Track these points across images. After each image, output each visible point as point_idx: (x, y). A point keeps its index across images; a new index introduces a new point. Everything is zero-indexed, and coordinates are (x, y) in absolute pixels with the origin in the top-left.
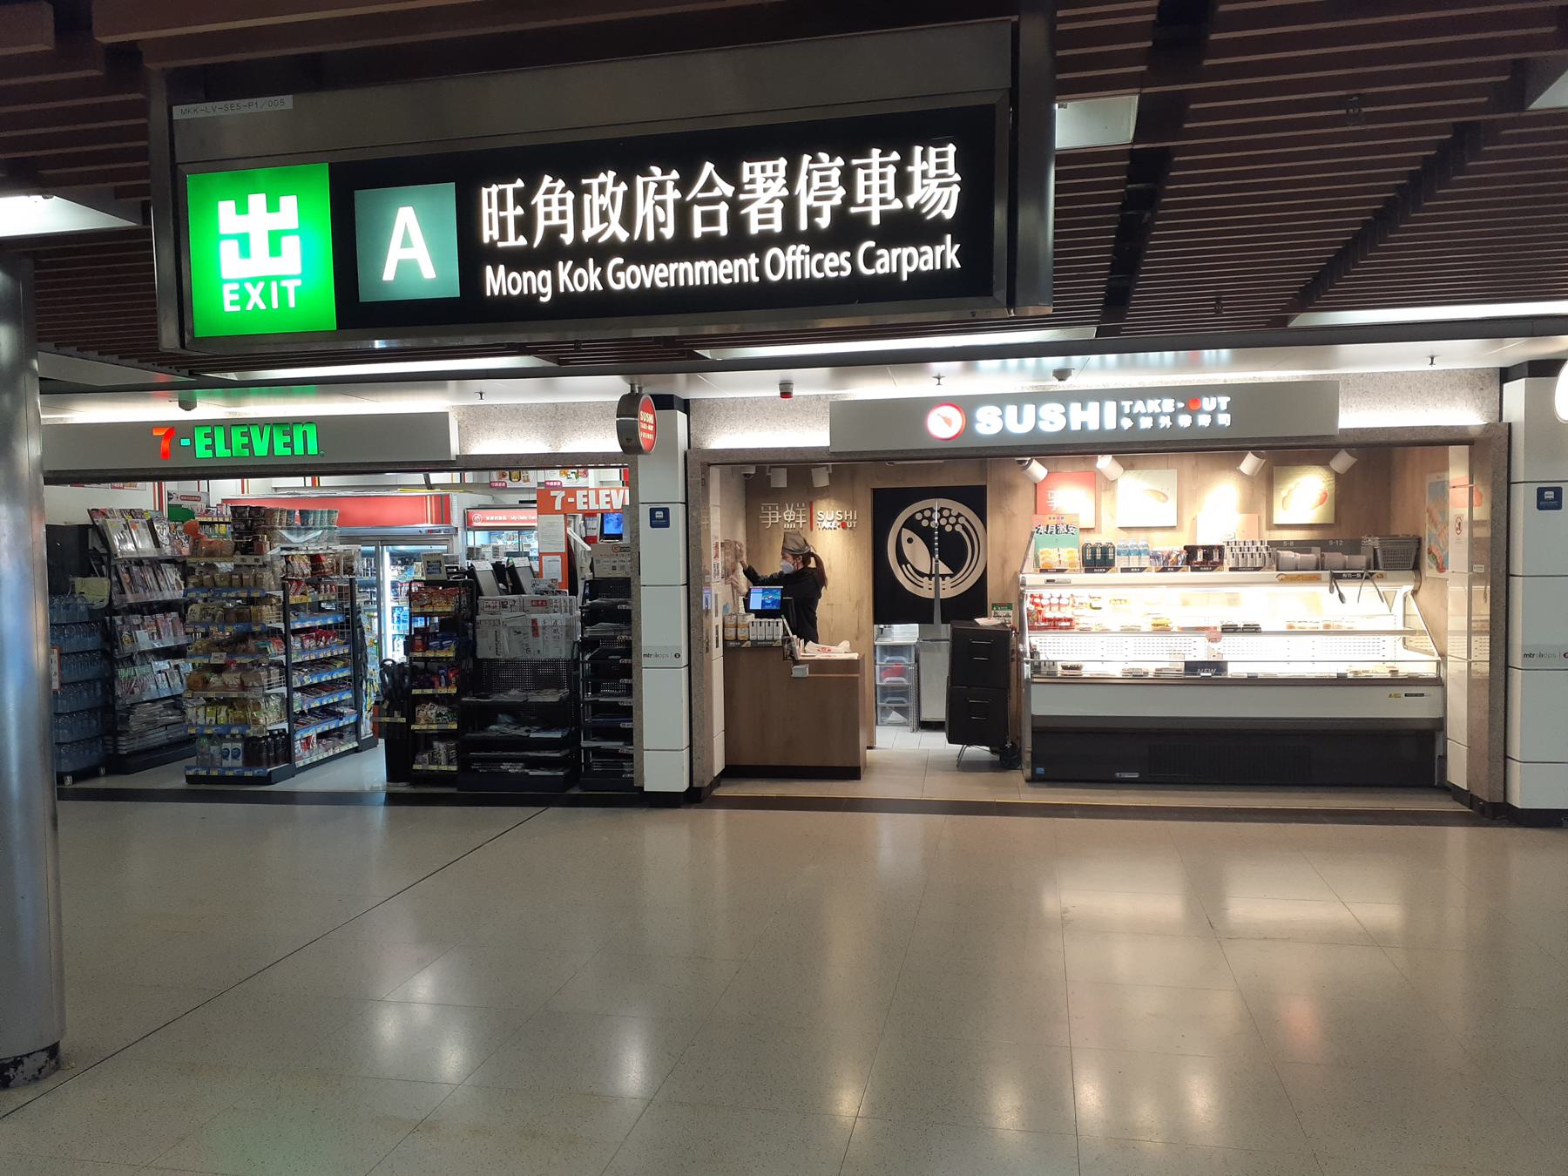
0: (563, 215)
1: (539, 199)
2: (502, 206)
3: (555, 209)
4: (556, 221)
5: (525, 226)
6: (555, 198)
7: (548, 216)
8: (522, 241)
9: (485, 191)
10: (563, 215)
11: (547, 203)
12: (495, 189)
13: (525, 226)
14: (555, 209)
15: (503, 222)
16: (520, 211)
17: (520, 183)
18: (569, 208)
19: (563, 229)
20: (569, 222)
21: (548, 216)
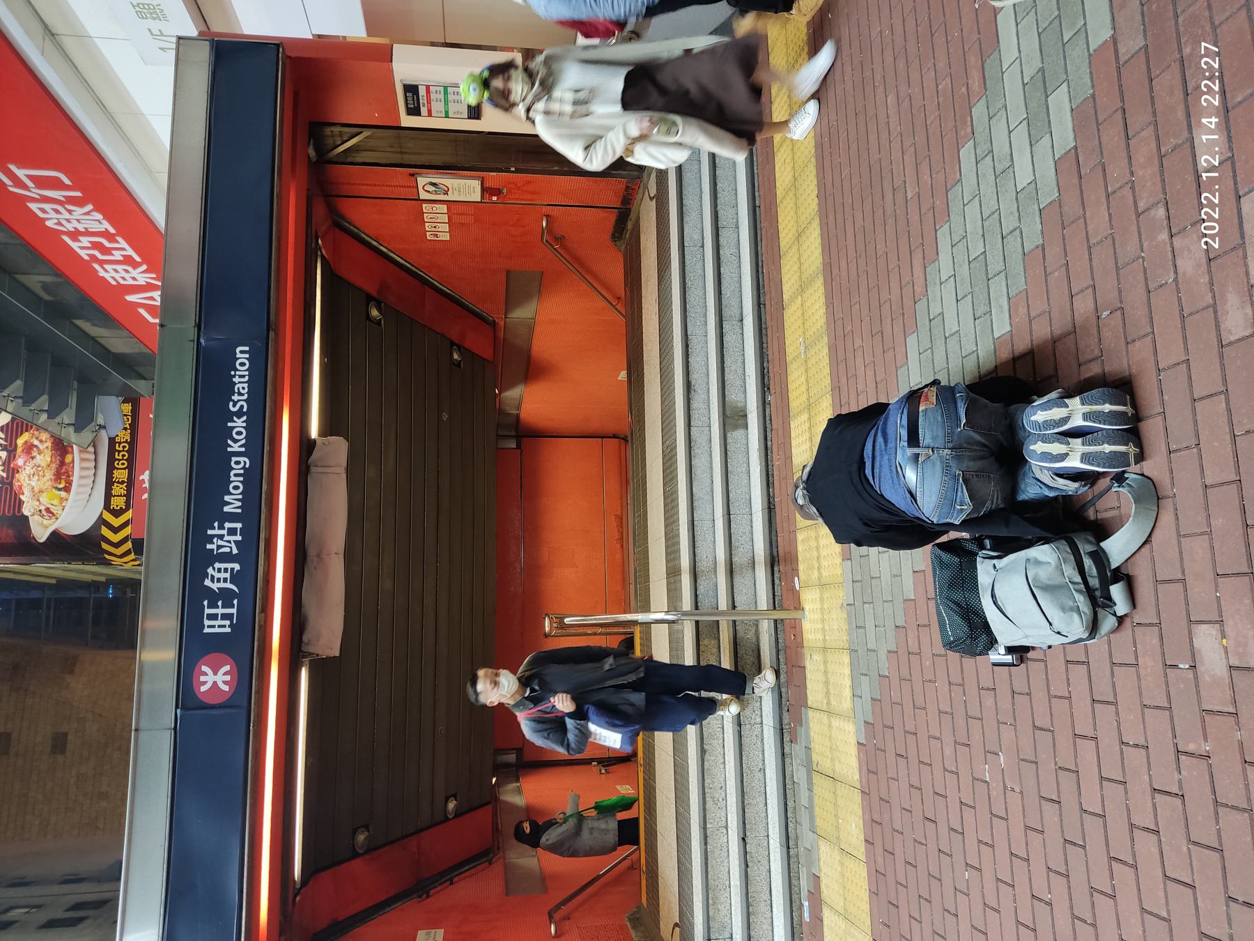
0: (226, 570)
1: (215, 586)
3: (222, 575)
4: (228, 575)
6: (217, 575)
7: (225, 580)
8: (235, 602)
9: (206, 630)
10: (226, 570)
11: (219, 580)
12: (207, 622)
14: (222, 575)
15: (224, 617)
16: (220, 603)
17: (206, 603)
18: (223, 566)
19: (232, 569)
20: (229, 566)
21: (225, 580)
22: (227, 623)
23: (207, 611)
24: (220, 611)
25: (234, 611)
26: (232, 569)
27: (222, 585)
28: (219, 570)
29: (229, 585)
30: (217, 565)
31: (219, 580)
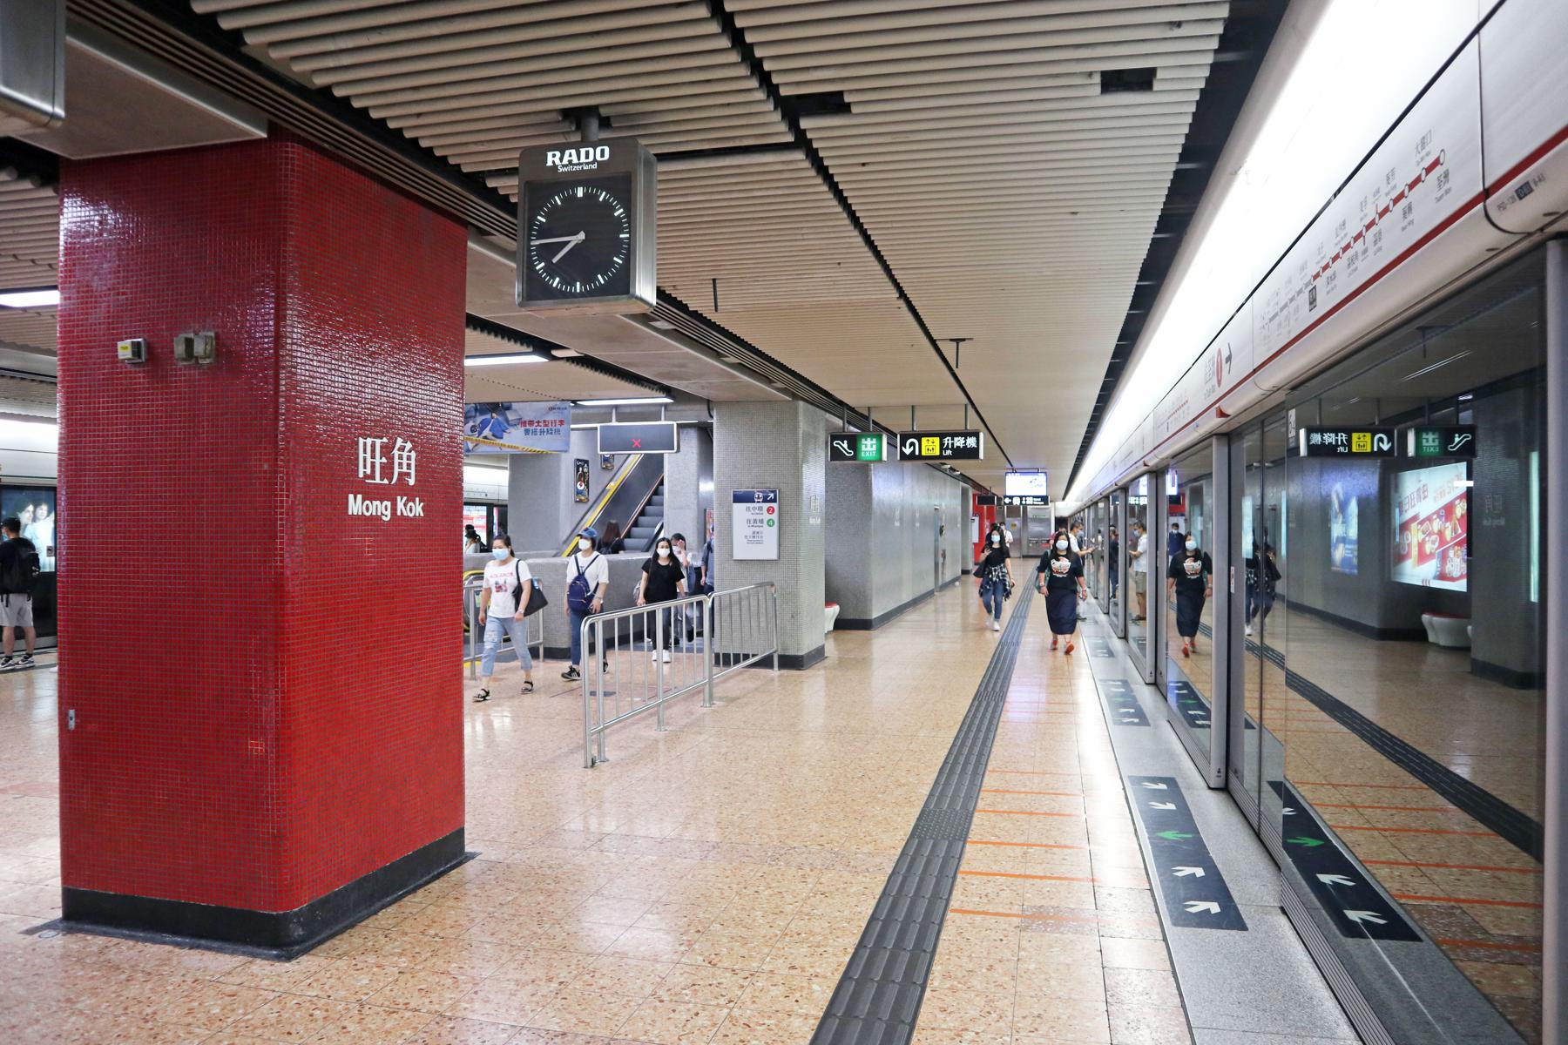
0: (409, 466)
2: (373, 457)
3: (405, 461)
4: (405, 470)
5: (387, 470)
10: (409, 466)
11: (401, 457)
12: (369, 441)
13: (387, 470)
14: (405, 461)
18: (413, 462)
20: (413, 472)
22: (368, 471)
23: (378, 442)
24: (378, 461)
25: (378, 480)
26: (408, 475)
27: (397, 461)
28: (409, 458)
29: (396, 470)
30: (413, 454)
31: (401, 457)
